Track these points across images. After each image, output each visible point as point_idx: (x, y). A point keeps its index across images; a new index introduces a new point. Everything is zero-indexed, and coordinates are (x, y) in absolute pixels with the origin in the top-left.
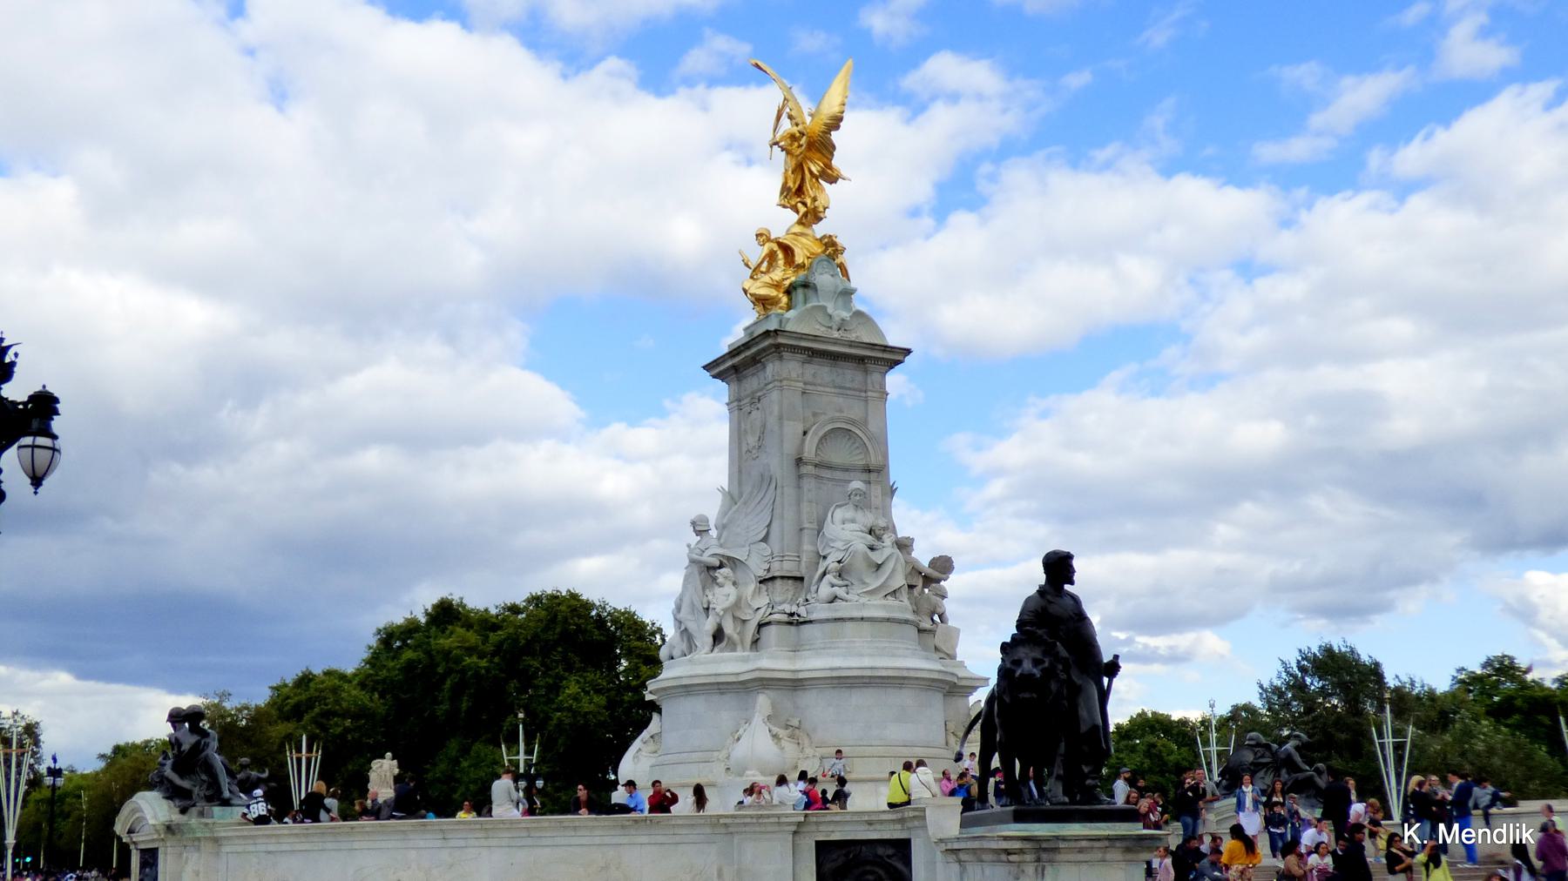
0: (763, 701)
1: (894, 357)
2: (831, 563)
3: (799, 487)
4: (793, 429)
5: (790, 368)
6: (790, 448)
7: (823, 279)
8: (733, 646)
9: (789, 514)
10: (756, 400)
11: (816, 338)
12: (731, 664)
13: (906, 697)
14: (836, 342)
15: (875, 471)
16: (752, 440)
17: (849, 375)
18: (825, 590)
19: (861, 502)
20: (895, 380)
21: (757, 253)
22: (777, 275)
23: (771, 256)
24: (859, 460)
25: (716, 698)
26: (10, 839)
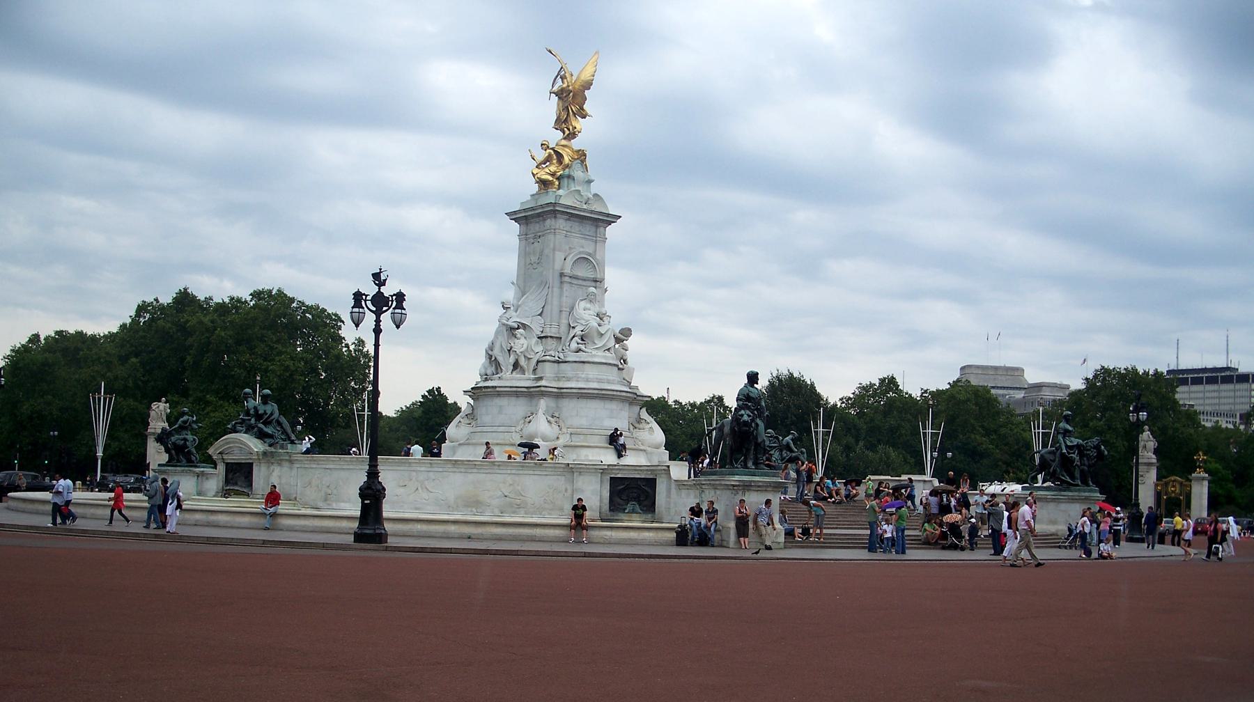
0: (543, 403)
1: (610, 219)
3: (561, 288)
5: (561, 223)
7: (578, 173)
9: (556, 302)
10: (537, 237)
11: (575, 208)
12: (523, 381)
13: (613, 406)
14: (584, 210)
15: (597, 282)
16: (534, 259)
17: (588, 229)
18: (574, 345)
19: (591, 299)
20: (611, 230)
21: (541, 155)
22: (553, 168)
24: (590, 275)
25: (513, 399)
26: (100, 454)
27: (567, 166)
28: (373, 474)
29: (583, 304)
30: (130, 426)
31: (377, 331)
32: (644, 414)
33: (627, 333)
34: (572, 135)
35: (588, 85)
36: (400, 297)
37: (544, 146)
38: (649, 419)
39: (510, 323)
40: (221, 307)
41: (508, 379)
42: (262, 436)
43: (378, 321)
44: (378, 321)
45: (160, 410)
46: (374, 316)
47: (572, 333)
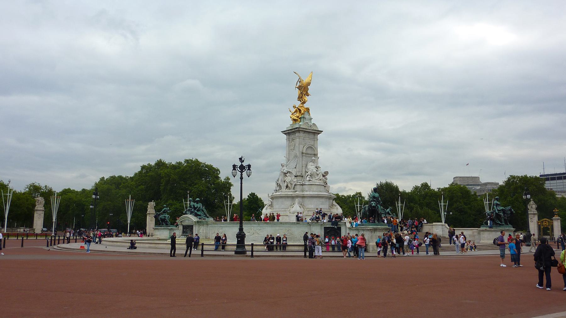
0: (297, 200)
2: (309, 173)
4: (301, 146)
5: (301, 134)
6: (301, 150)
7: (307, 116)
9: (300, 163)
10: (293, 140)
12: (290, 193)
13: (323, 200)
15: (315, 155)
16: (292, 148)
17: (311, 136)
18: (308, 179)
19: (313, 161)
21: (294, 110)
22: (298, 115)
23: (296, 111)
24: (313, 153)
27: (303, 114)
28: (241, 229)
29: (310, 164)
31: (241, 178)
32: (334, 203)
33: (327, 173)
34: (304, 103)
35: (309, 84)
36: (249, 166)
37: (294, 107)
41: (284, 192)
42: (196, 215)
43: (242, 175)
44: (242, 175)
45: (151, 205)
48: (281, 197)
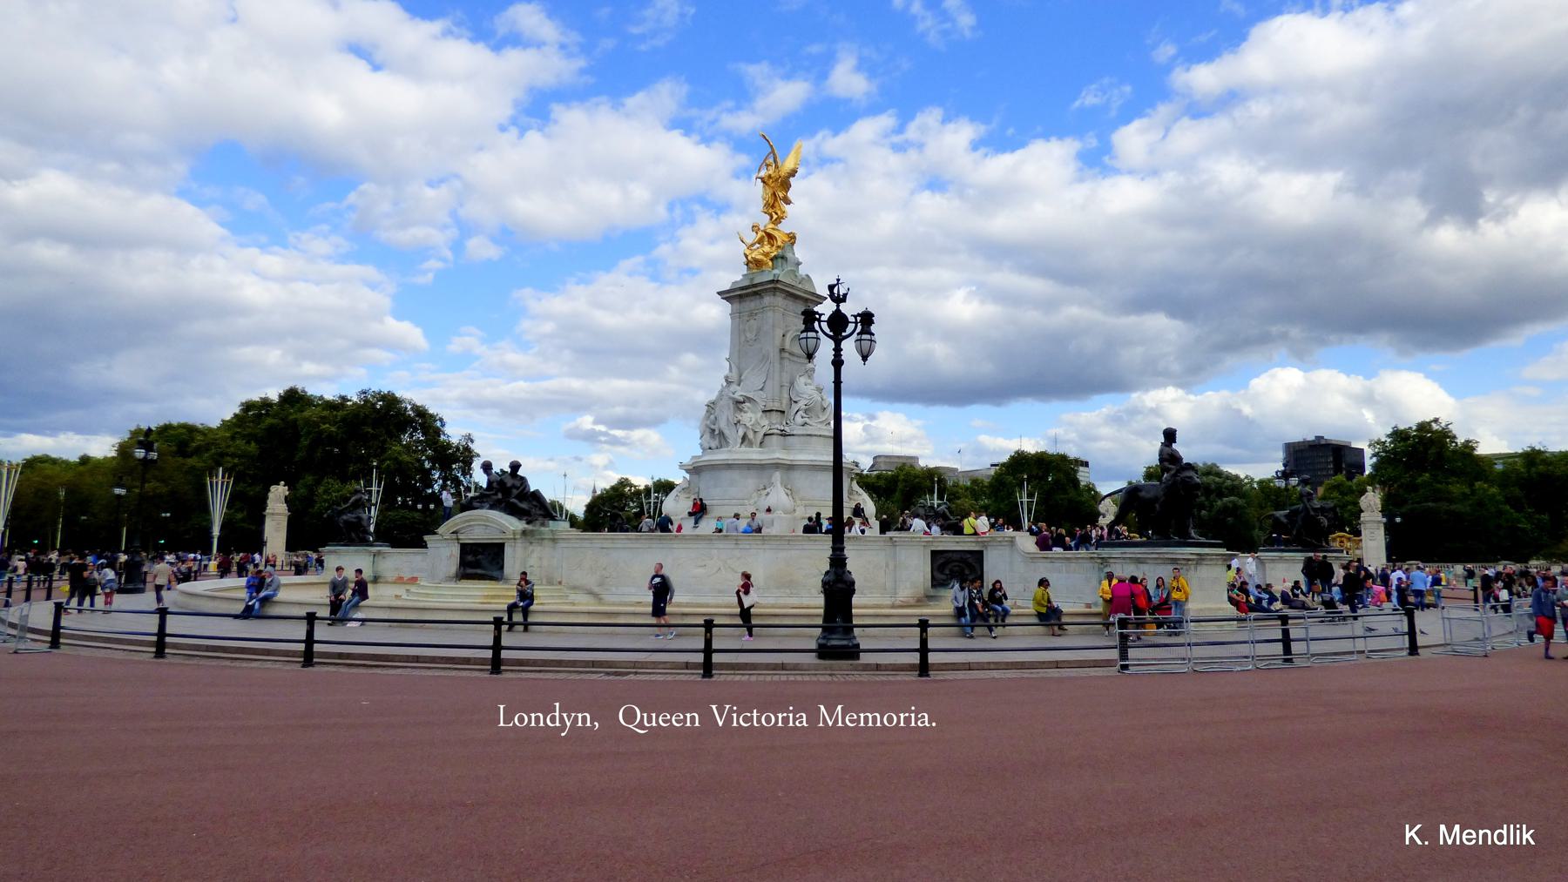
2: (801, 404)
5: (779, 300)
8: (751, 444)
10: (752, 314)
18: (799, 420)
21: (751, 237)
22: (767, 248)
28: (838, 561)
29: (803, 380)
30: (248, 511)
31: (838, 363)
34: (778, 221)
36: (867, 319)
37: (755, 228)
38: (861, 491)
39: (736, 396)
40: (330, 406)
41: (736, 453)
43: (838, 350)
44: (838, 350)
45: (278, 492)
46: (832, 344)
47: (795, 407)
48: (729, 466)
